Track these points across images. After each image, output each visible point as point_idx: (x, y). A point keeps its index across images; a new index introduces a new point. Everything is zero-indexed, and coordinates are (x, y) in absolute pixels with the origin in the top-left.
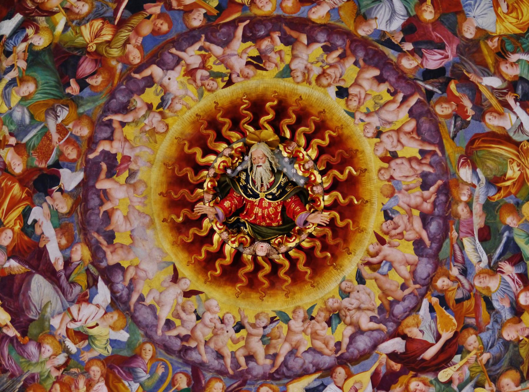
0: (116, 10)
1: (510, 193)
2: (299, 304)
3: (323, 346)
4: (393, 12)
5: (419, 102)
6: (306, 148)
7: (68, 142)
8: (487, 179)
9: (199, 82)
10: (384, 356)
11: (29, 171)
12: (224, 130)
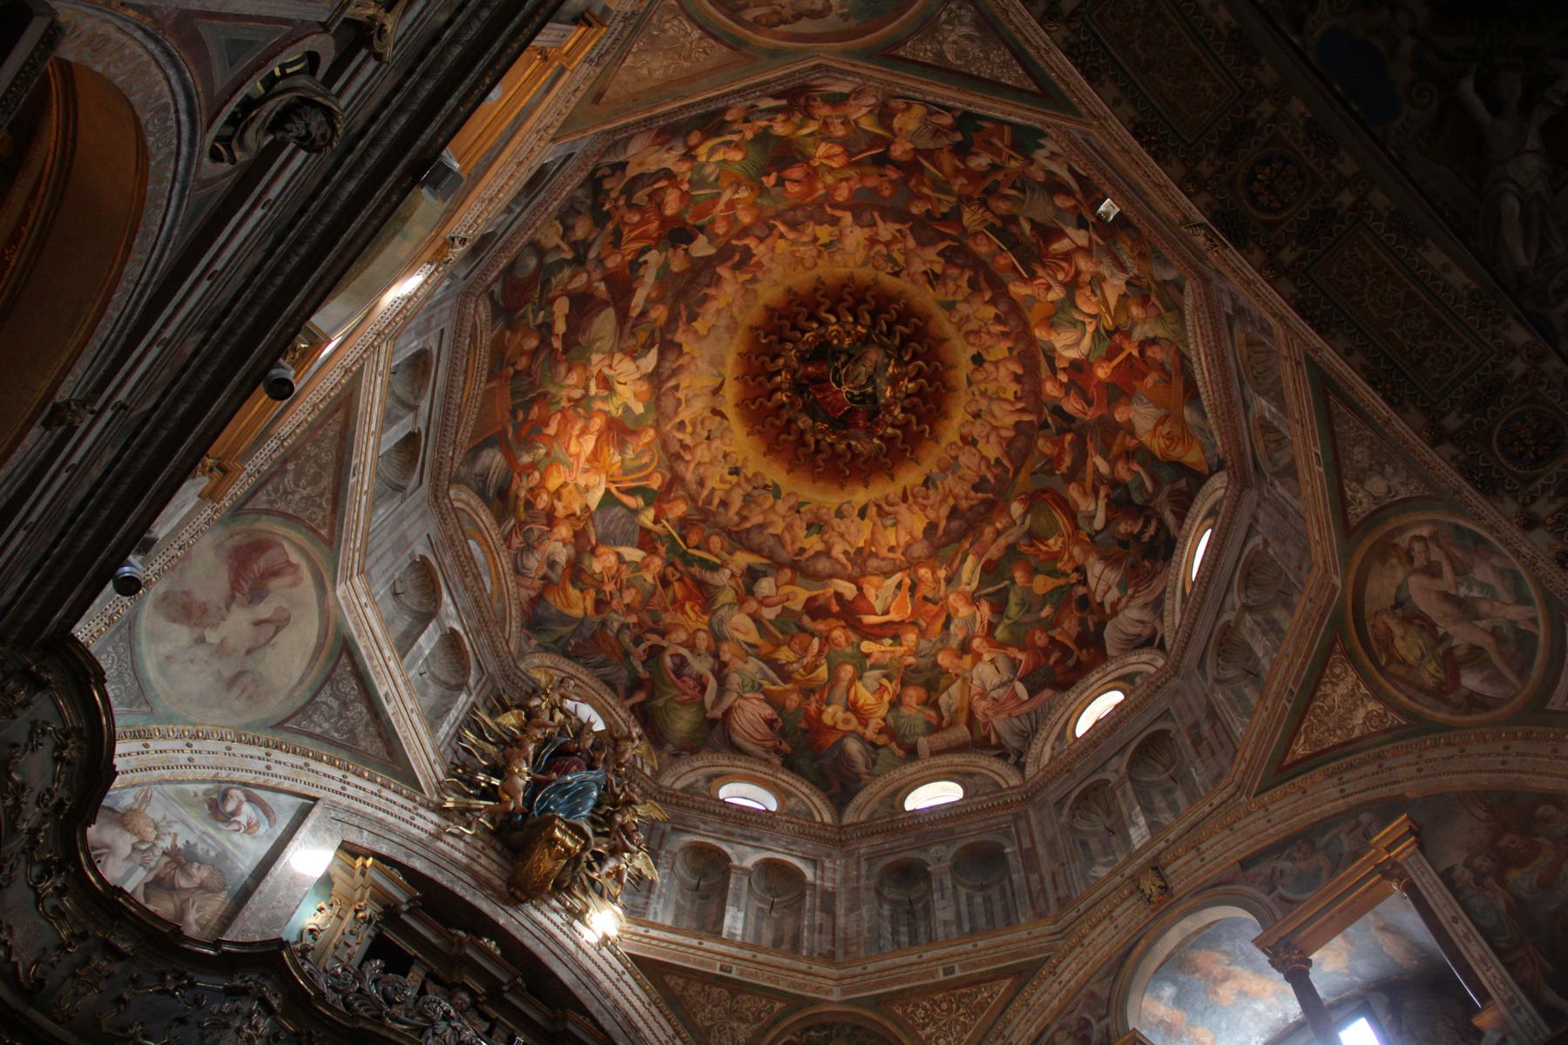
0: (864, 151)
3: (789, 541)
4: (1077, 344)
5: (1031, 422)
6: (910, 381)
7: (726, 218)
8: (1030, 529)
9: (872, 254)
10: (832, 590)
11: (677, 218)
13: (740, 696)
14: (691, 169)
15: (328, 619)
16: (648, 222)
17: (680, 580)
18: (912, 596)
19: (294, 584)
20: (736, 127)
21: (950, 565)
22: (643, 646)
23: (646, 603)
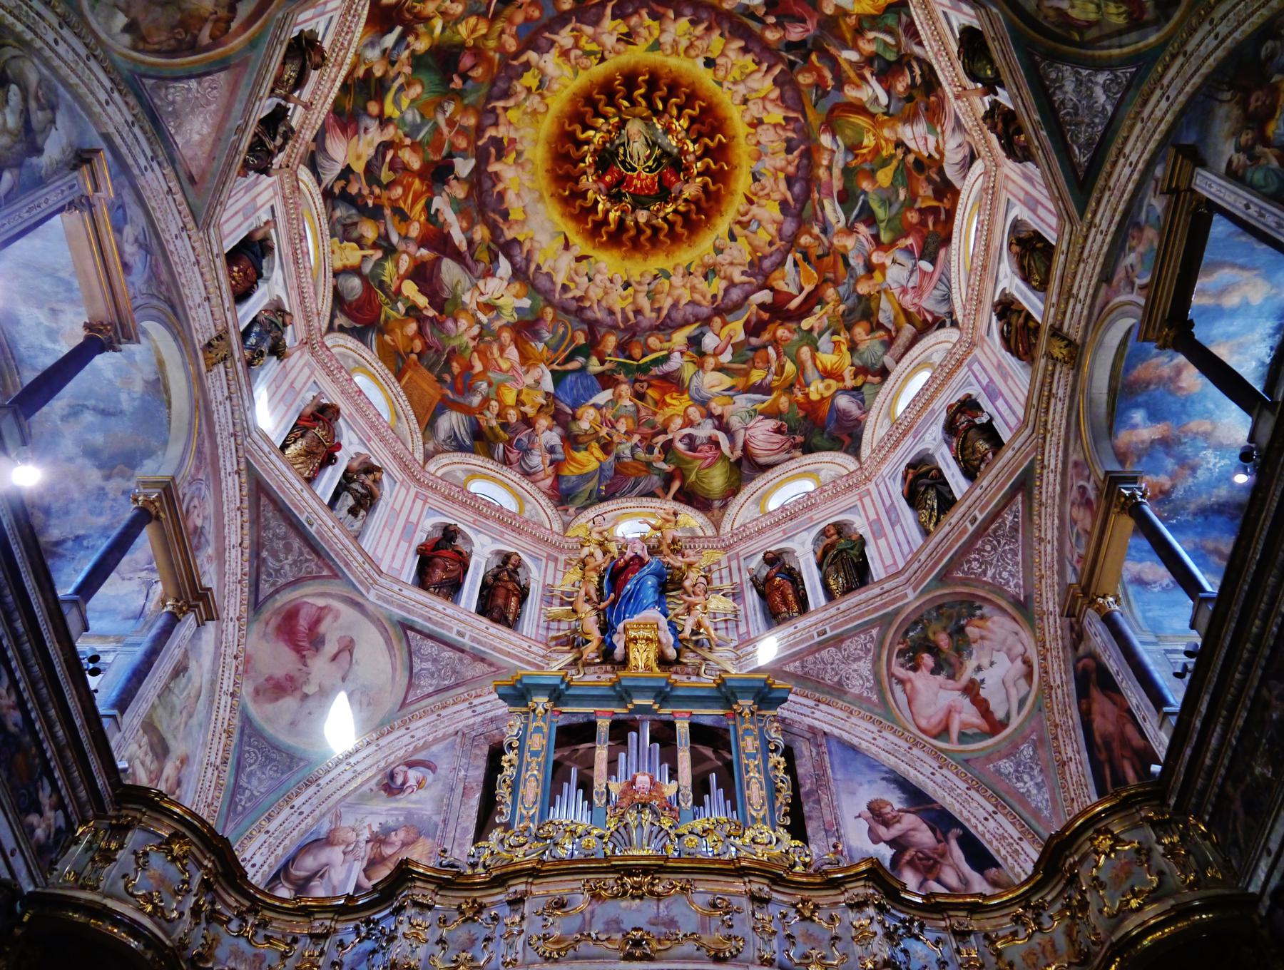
1: (865, 161)
2: (678, 261)
5: (782, 71)
6: (678, 119)
7: (458, 133)
9: (573, 62)
11: (426, 165)
12: (601, 105)
13: (746, 429)
14: (397, 128)
16: (411, 185)
17: (650, 386)
18: (809, 263)
19: (336, 617)
20: (392, 73)
21: (817, 220)
22: (656, 450)
23: (638, 421)
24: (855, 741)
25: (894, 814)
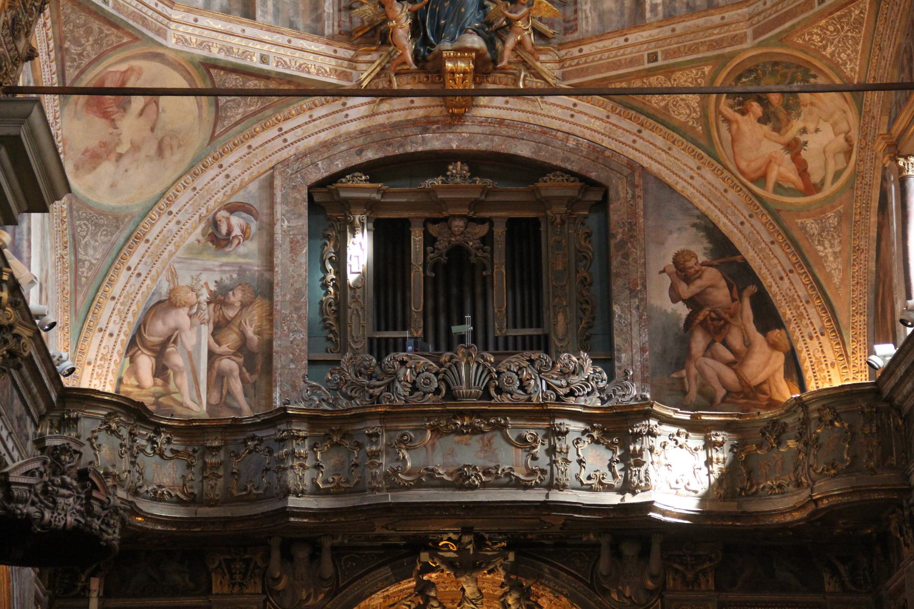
15: (180, 64)
24: (670, 179)
25: (697, 268)
